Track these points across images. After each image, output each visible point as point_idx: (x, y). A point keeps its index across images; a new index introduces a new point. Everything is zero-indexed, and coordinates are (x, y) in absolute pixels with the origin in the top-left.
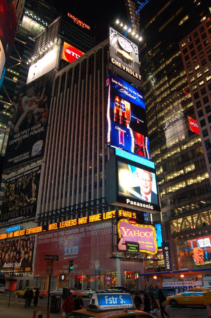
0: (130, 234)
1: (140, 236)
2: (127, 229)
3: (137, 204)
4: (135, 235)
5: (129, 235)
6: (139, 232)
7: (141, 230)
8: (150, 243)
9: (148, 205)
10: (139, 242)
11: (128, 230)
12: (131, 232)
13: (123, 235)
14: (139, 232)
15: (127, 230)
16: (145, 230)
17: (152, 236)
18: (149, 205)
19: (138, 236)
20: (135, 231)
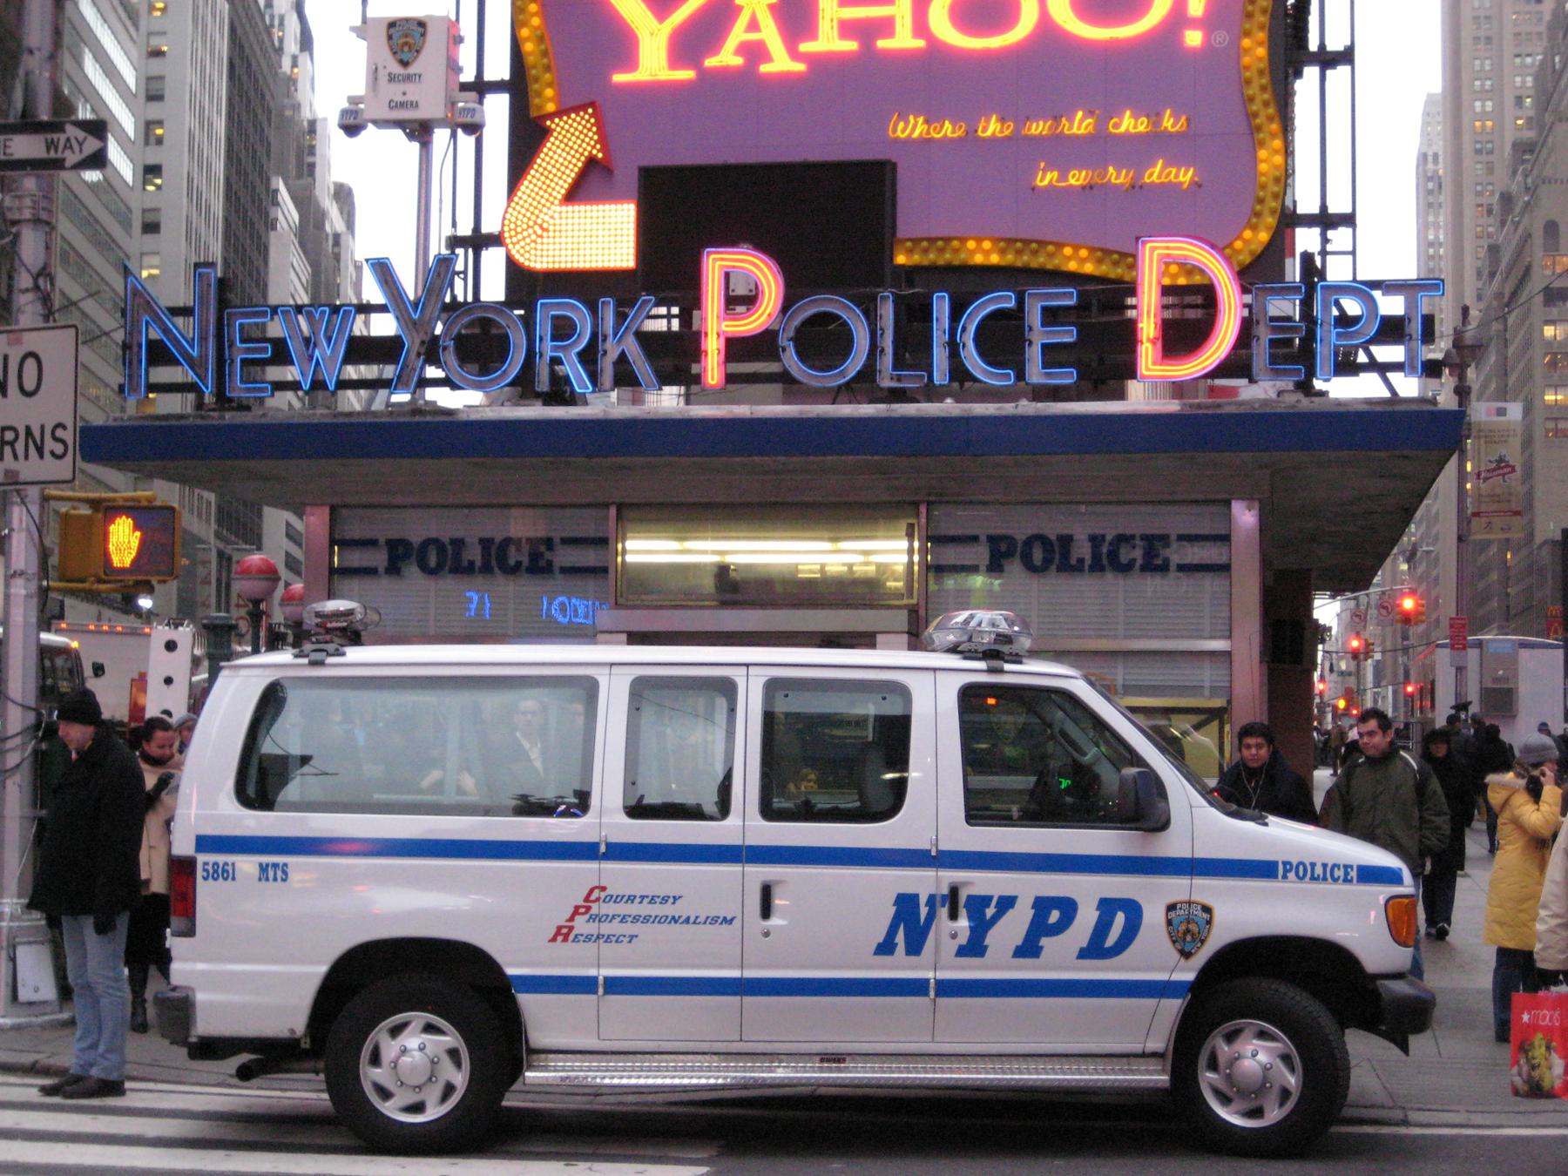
0: (738, 34)
1: (934, 44)
4: (828, 41)
5: (727, 57)
8: (1129, 124)
19: (903, 39)
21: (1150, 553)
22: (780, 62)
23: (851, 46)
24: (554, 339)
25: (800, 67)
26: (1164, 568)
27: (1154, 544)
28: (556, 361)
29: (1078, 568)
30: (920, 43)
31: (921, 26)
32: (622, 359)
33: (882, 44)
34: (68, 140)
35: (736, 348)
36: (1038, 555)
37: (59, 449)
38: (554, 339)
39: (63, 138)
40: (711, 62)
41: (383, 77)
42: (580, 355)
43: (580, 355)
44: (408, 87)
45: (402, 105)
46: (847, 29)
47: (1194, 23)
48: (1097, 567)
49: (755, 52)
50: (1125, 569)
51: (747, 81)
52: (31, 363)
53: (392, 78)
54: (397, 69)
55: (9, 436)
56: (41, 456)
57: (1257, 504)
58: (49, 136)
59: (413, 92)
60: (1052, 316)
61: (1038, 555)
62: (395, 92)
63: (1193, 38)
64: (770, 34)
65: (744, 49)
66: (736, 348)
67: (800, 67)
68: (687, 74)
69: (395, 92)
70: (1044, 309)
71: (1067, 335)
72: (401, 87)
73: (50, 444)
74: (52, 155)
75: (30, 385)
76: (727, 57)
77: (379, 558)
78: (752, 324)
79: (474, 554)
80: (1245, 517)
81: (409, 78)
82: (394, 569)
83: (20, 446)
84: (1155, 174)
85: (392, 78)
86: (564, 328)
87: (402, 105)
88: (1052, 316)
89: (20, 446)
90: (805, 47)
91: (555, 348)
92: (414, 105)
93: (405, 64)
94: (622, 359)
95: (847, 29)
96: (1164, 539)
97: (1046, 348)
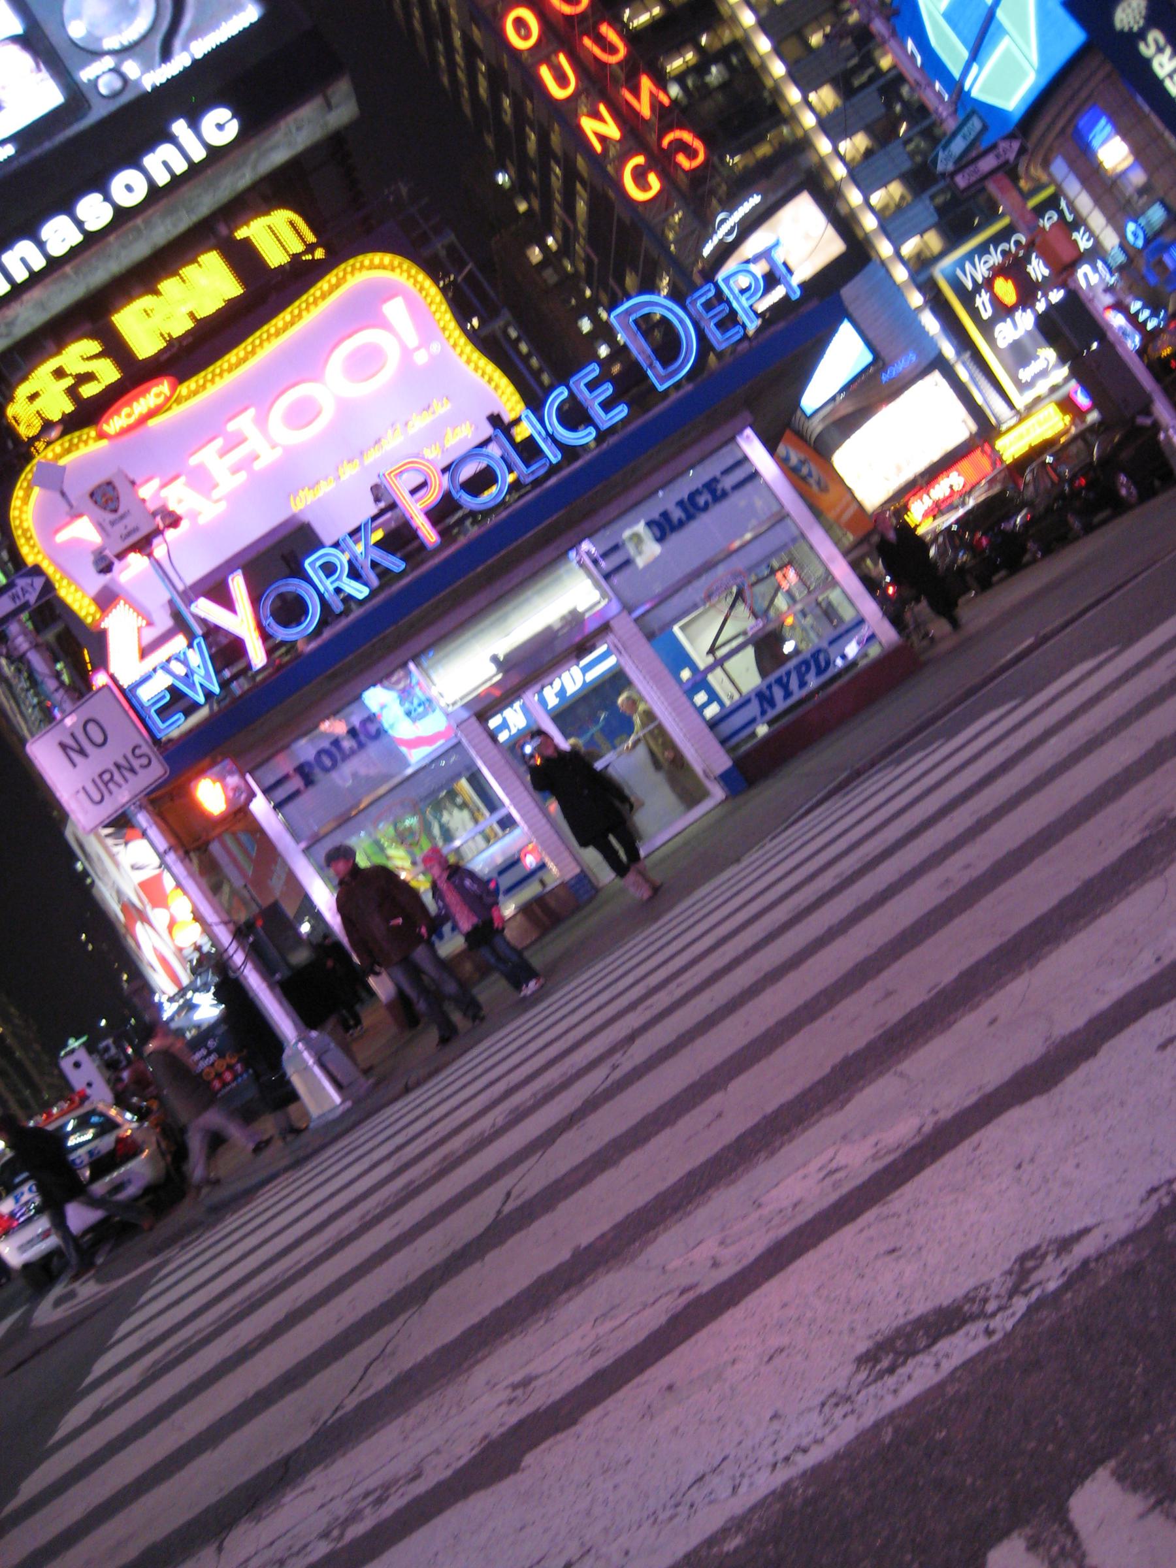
1: (287, 450)
3: (41, 245)
6: (261, 421)
7: (257, 395)
9: (166, 151)
10: (301, 504)
14: (261, 421)
16: (305, 361)
17: (412, 339)
18: (172, 139)
19: (268, 457)
20: (208, 456)
21: (713, 492)
23: (242, 476)
24: (328, 576)
26: (725, 494)
27: (710, 486)
29: (681, 524)
30: (278, 452)
32: (374, 564)
34: (22, 589)
37: (145, 761)
38: (328, 576)
41: (108, 527)
42: (349, 576)
43: (349, 576)
45: (129, 535)
46: (235, 470)
48: (690, 517)
53: (113, 523)
54: (112, 516)
58: (10, 593)
59: (130, 522)
60: (592, 386)
62: (120, 529)
63: (421, 358)
67: (222, 506)
69: (120, 529)
70: (587, 385)
71: (607, 390)
73: (136, 764)
74: (19, 603)
75: (99, 738)
77: (296, 783)
81: (122, 517)
83: (117, 777)
85: (113, 523)
86: (329, 569)
87: (129, 535)
88: (592, 386)
89: (117, 777)
90: (216, 494)
91: (332, 583)
92: (136, 530)
93: (115, 511)
94: (374, 564)
95: (235, 470)
96: (715, 480)
97: (602, 405)
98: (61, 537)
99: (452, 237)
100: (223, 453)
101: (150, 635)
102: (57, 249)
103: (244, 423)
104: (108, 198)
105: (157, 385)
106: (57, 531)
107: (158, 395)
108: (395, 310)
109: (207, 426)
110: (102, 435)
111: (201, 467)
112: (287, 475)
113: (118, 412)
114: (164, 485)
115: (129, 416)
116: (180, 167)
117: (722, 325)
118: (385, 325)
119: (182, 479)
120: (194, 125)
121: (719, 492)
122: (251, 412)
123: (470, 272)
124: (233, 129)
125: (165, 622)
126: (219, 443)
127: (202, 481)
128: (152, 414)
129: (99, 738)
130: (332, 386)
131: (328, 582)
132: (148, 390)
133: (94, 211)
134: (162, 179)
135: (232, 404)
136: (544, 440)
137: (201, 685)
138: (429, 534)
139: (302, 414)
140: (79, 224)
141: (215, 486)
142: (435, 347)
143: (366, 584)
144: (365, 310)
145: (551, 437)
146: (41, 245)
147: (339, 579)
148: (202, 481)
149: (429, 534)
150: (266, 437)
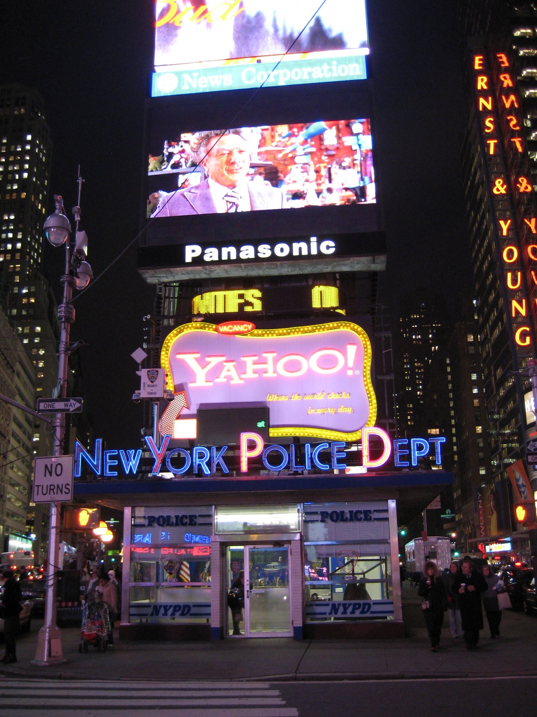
0: (224, 373)
1: (279, 377)
2: (208, 359)
3: (238, 252)
4: (250, 374)
5: (221, 379)
6: (276, 361)
7: (281, 350)
9: (303, 245)
10: (271, 399)
11: (214, 361)
12: (230, 366)
13: (191, 385)
14: (276, 361)
15: (209, 363)
16: (306, 348)
17: (351, 364)
18: (308, 243)
19: (270, 374)
20: (249, 360)
22: (236, 381)
23: (256, 376)
24: (199, 458)
25: (242, 382)
27: (367, 513)
28: (199, 465)
30: (275, 375)
31: (275, 371)
32: (218, 465)
33: (265, 375)
35: (251, 461)
36: (335, 517)
37: (67, 491)
38: (199, 458)
39: (69, 403)
40: (217, 380)
41: (146, 386)
42: (206, 463)
43: (206, 463)
44: (153, 388)
45: (151, 393)
46: (255, 372)
47: (350, 369)
48: (351, 520)
49: (229, 378)
50: (359, 520)
51: (227, 386)
52: (59, 467)
53: (149, 386)
54: (150, 384)
55: (52, 487)
56: (62, 493)
57: (395, 500)
59: (154, 389)
61: (335, 517)
63: (350, 373)
64: (233, 373)
65: (225, 377)
66: (251, 461)
67: (242, 382)
68: (211, 384)
72: (150, 388)
74: (66, 408)
75: (58, 473)
76: (221, 379)
78: (255, 453)
79: (174, 520)
80: (392, 504)
81: (153, 386)
82: (150, 525)
83: (55, 490)
84: (341, 410)
86: (201, 456)
87: (151, 393)
89: (55, 490)
90: (243, 376)
91: (199, 461)
92: (155, 393)
93: (152, 382)
94: (218, 465)
95: (255, 372)
97: (338, 459)
98: (179, 356)
99: (390, 335)
100: (255, 363)
101: (185, 411)
102: (243, 256)
103: (270, 357)
104: (272, 249)
105: (247, 324)
106: (179, 353)
107: (245, 328)
108: (352, 350)
109: (256, 350)
110: (217, 330)
111: (245, 362)
112: (273, 385)
113: (227, 325)
114: (226, 361)
115: (231, 329)
116: (305, 252)
117: (402, 458)
118: (344, 353)
119: (234, 363)
120: (319, 243)
121: (369, 517)
122: (275, 355)
123: (389, 352)
124: (332, 251)
125: (194, 410)
126: (256, 358)
127: (241, 369)
128: (239, 333)
129: (58, 473)
130: (311, 363)
131: (198, 460)
132: (242, 324)
133: (264, 251)
134: (296, 253)
135: (270, 348)
136: (308, 458)
137: (131, 467)
138: (244, 467)
139: (292, 367)
140: (256, 252)
141: (245, 373)
142: (357, 372)
143: (210, 470)
144: (339, 343)
145: (312, 459)
146: (238, 252)
147: (202, 461)
148: (241, 369)
149: (244, 467)
150: (274, 367)
